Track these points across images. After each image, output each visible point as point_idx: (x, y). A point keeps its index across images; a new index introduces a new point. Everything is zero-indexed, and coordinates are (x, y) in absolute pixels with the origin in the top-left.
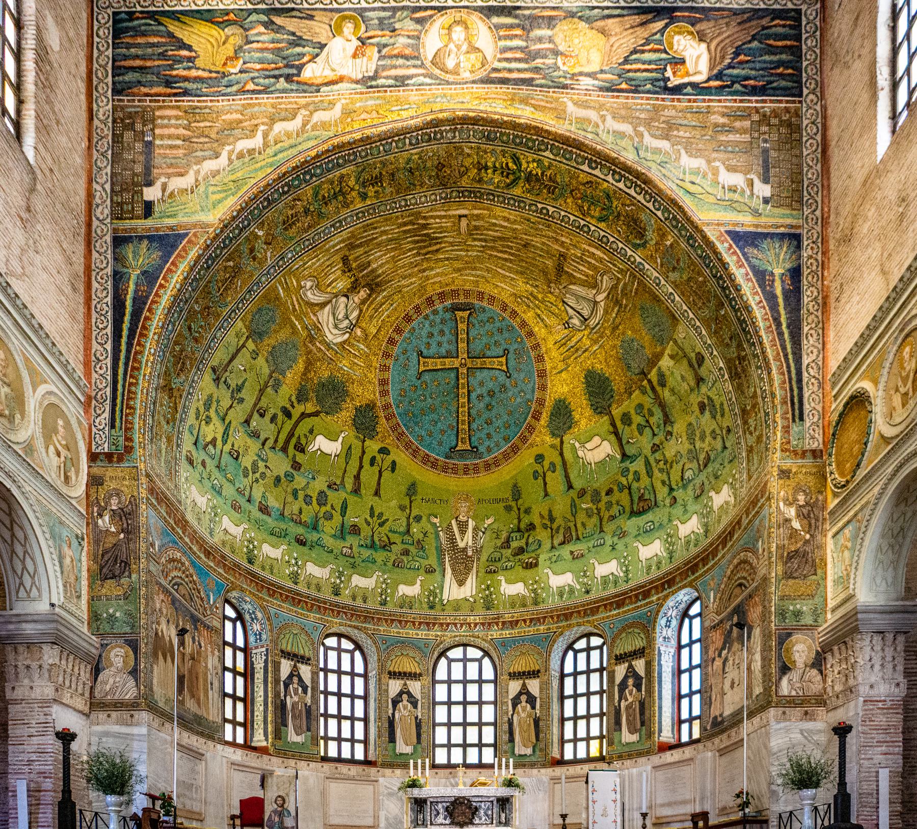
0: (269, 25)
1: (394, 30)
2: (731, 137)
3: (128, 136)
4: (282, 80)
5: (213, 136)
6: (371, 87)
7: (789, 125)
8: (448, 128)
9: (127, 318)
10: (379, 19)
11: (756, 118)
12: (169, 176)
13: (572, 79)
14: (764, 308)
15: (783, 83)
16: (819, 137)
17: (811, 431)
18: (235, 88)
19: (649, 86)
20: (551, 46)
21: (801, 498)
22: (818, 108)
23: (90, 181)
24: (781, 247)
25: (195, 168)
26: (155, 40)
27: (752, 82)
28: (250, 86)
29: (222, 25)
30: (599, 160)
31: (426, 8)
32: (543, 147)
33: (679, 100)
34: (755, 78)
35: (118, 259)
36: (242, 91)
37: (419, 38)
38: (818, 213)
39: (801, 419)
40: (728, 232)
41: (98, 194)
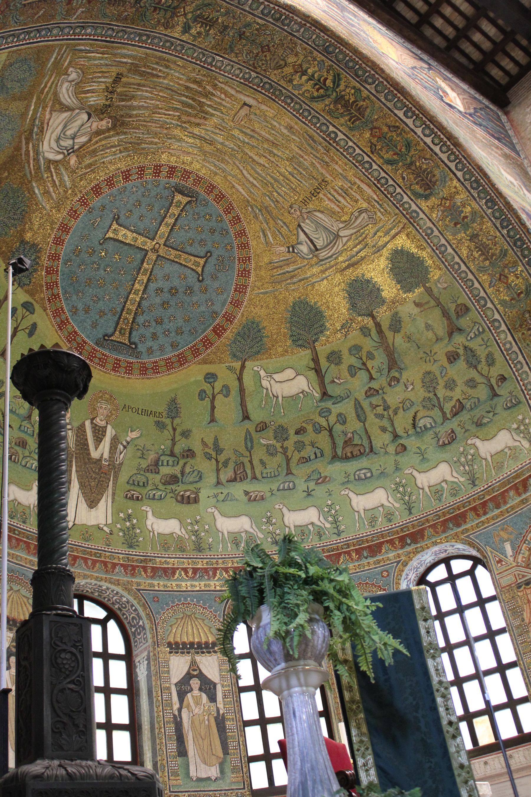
8: (299, 20)
30: (417, 112)
32: (370, 80)
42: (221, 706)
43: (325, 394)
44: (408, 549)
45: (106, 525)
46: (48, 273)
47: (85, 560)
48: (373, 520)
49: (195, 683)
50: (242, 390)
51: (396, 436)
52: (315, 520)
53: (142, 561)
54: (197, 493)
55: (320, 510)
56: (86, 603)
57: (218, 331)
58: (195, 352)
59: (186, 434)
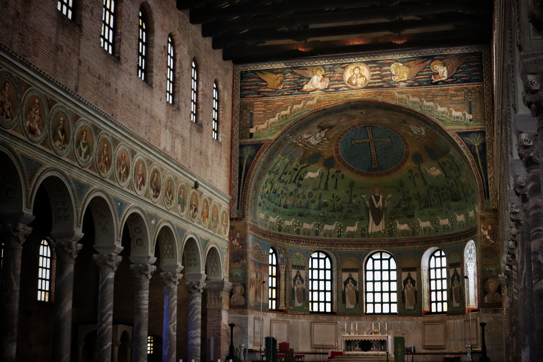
0: (292, 73)
1: (334, 72)
2: (457, 98)
3: (245, 111)
4: (296, 90)
5: (273, 110)
6: (327, 92)
7: (479, 91)
9: (244, 172)
10: (329, 68)
11: (466, 91)
12: (258, 124)
13: (397, 83)
14: (472, 158)
15: (476, 77)
16: (491, 96)
17: (493, 202)
18: (280, 94)
19: (425, 83)
20: (390, 73)
21: (490, 227)
22: (490, 85)
23: (232, 126)
24: (477, 136)
25: (267, 121)
26: (254, 80)
27: (464, 78)
28: (286, 93)
29: (276, 74)
31: (345, 63)
33: (437, 87)
34: (465, 77)
35: (241, 152)
36: (283, 95)
37: (343, 74)
38: (491, 123)
39: (488, 197)
40: (456, 133)
41: (235, 131)
42: (416, 288)
43: (446, 175)
44: (467, 239)
45: (383, 230)
46: (339, 161)
47: (375, 244)
48: (460, 226)
49: (409, 281)
50: (422, 174)
51: (465, 195)
52: (447, 223)
53: (394, 241)
54: (413, 213)
55: (449, 220)
56: (383, 253)
57: (407, 156)
58: (403, 164)
59: (408, 192)
